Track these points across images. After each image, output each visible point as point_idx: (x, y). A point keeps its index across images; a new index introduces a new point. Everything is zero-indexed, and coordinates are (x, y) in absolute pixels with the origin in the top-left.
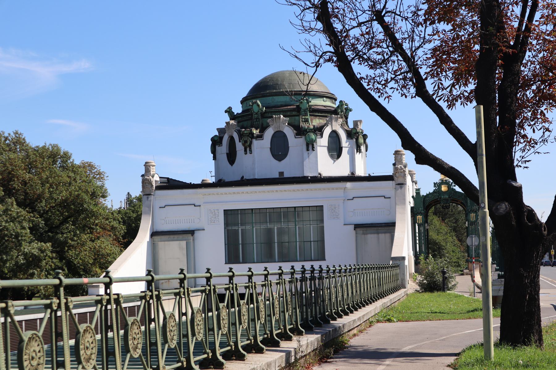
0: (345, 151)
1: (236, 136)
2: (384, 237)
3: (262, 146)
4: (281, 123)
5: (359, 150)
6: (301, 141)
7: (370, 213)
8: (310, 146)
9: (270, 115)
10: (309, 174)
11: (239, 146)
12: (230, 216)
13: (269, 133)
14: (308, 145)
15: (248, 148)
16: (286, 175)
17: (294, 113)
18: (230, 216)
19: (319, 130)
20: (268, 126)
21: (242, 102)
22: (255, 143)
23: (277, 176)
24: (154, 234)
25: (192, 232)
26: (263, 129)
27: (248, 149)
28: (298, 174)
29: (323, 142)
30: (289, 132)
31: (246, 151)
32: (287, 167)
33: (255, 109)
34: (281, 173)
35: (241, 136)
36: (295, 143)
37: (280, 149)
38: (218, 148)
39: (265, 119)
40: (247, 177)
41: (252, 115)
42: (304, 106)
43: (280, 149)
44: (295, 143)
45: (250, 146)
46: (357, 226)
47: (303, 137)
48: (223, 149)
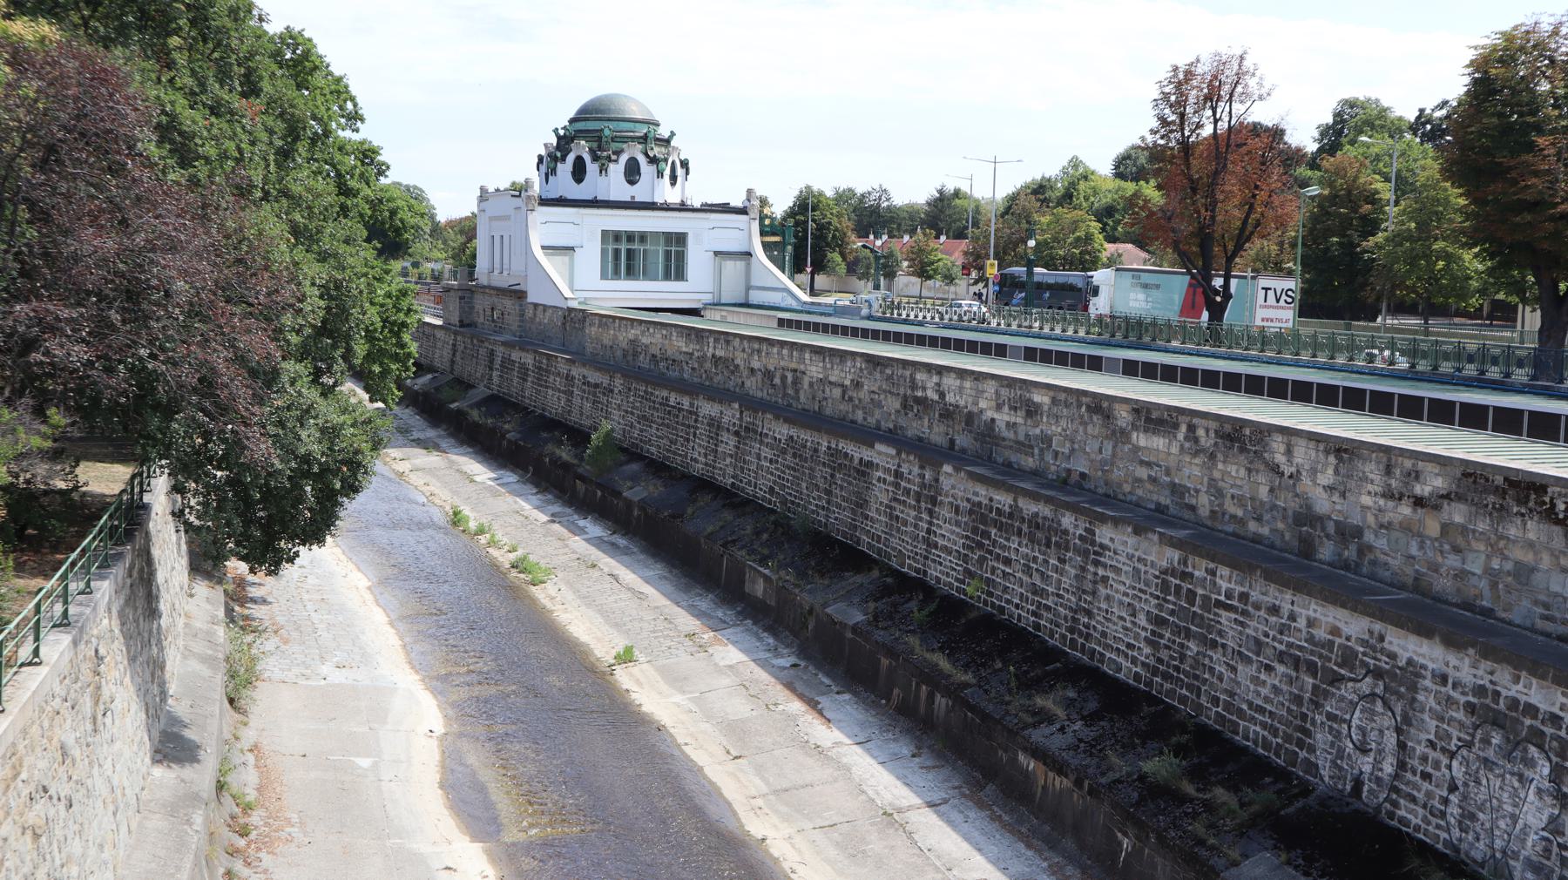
1: (587, 158)
2: (740, 265)
3: (617, 170)
4: (636, 151)
7: (733, 243)
8: (660, 174)
10: (659, 200)
11: (592, 168)
12: (605, 233)
13: (624, 158)
15: (603, 170)
16: (637, 199)
18: (605, 233)
19: (666, 160)
21: (572, 121)
22: (612, 166)
24: (543, 248)
25: (572, 249)
26: (618, 153)
28: (649, 200)
29: (667, 172)
30: (642, 159)
32: (640, 192)
33: (607, 132)
35: (595, 158)
36: (646, 169)
37: (632, 173)
42: (651, 135)
43: (632, 173)
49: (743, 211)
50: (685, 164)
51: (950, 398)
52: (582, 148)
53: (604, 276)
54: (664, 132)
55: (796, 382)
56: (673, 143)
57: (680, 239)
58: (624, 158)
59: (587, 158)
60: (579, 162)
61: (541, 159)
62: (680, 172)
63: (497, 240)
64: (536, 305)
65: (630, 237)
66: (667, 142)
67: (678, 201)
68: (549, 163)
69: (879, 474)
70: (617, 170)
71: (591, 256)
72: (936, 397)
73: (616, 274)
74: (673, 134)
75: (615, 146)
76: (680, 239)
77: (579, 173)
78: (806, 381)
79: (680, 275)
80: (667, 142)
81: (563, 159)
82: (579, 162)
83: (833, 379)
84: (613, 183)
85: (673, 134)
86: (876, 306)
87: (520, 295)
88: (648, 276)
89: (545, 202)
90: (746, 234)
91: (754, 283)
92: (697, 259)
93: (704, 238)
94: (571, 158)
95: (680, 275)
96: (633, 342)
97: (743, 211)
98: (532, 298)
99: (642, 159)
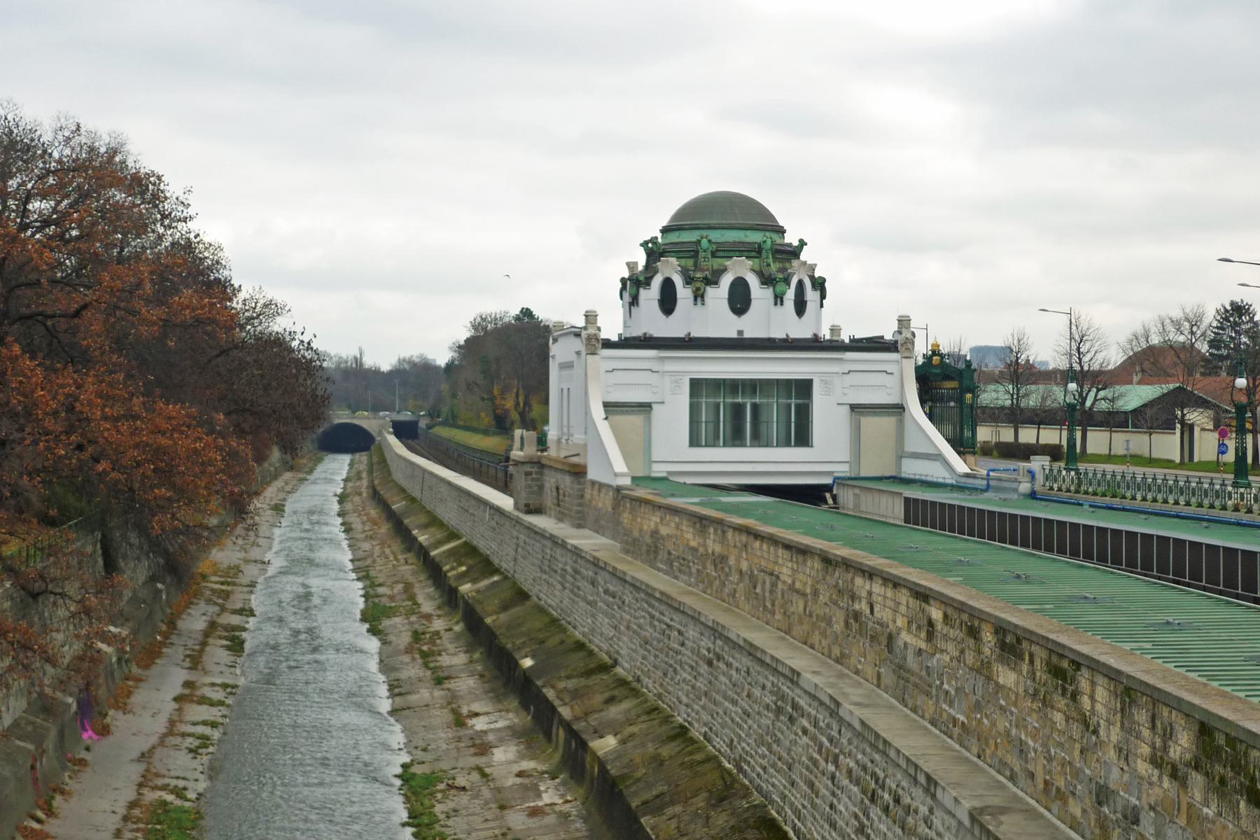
0: (811, 306)
1: (678, 280)
2: (888, 422)
3: (719, 295)
5: (822, 306)
6: (768, 293)
8: (779, 299)
9: (721, 254)
10: (779, 334)
11: (684, 293)
13: (726, 280)
14: (776, 297)
15: (699, 296)
16: (747, 335)
17: (753, 254)
19: (787, 281)
20: (724, 270)
21: (665, 231)
22: (711, 292)
23: (735, 335)
24: (607, 405)
27: (699, 299)
29: (790, 294)
30: (753, 281)
31: (695, 300)
32: (752, 325)
33: (704, 243)
34: (740, 332)
35: (688, 281)
36: (759, 294)
37: (740, 301)
38: (643, 293)
39: (719, 260)
40: (696, 333)
41: (697, 252)
43: (740, 301)
44: (759, 294)
45: (702, 296)
46: (854, 408)
47: (771, 289)
48: (651, 295)
49: (891, 347)
50: (819, 285)
51: (877, 614)
52: (670, 268)
53: (694, 442)
54: (791, 238)
55: (774, 585)
56: (803, 257)
57: (804, 388)
58: (726, 280)
59: (678, 280)
60: (668, 285)
61: (623, 281)
62: (811, 295)
63: (565, 392)
64: (593, 483)
65: (734, 386)
66: (795, 252)
67: (809, 335)
68: (633, 285)
69: (805, 723)
70: (719, 295)
71: (674, 416)
72: (868, 611)
73: (713, 443)
74: (803, 243)
75: (716, 263)
76: (804, 388)
77: (668, 302)
78: (780, 585)
79: (803, 439)
80: (795, 252)
81: (647, 283)
82: (668, 285)
83: (798, 585)
84: (712, 315)
85: (803, 243)
86: (1040, 478)
87: (578, 472)
88: (759, 439)
89: (626, 343)
90: (895, 381)
91: (910, 447)
92: (827, 416)
93: (835, 390)
94: (657, 281)
95: (803, 439)
96: (655, 533)
97: (891, 347)
98: (593, 474)
99: (753, 281)
